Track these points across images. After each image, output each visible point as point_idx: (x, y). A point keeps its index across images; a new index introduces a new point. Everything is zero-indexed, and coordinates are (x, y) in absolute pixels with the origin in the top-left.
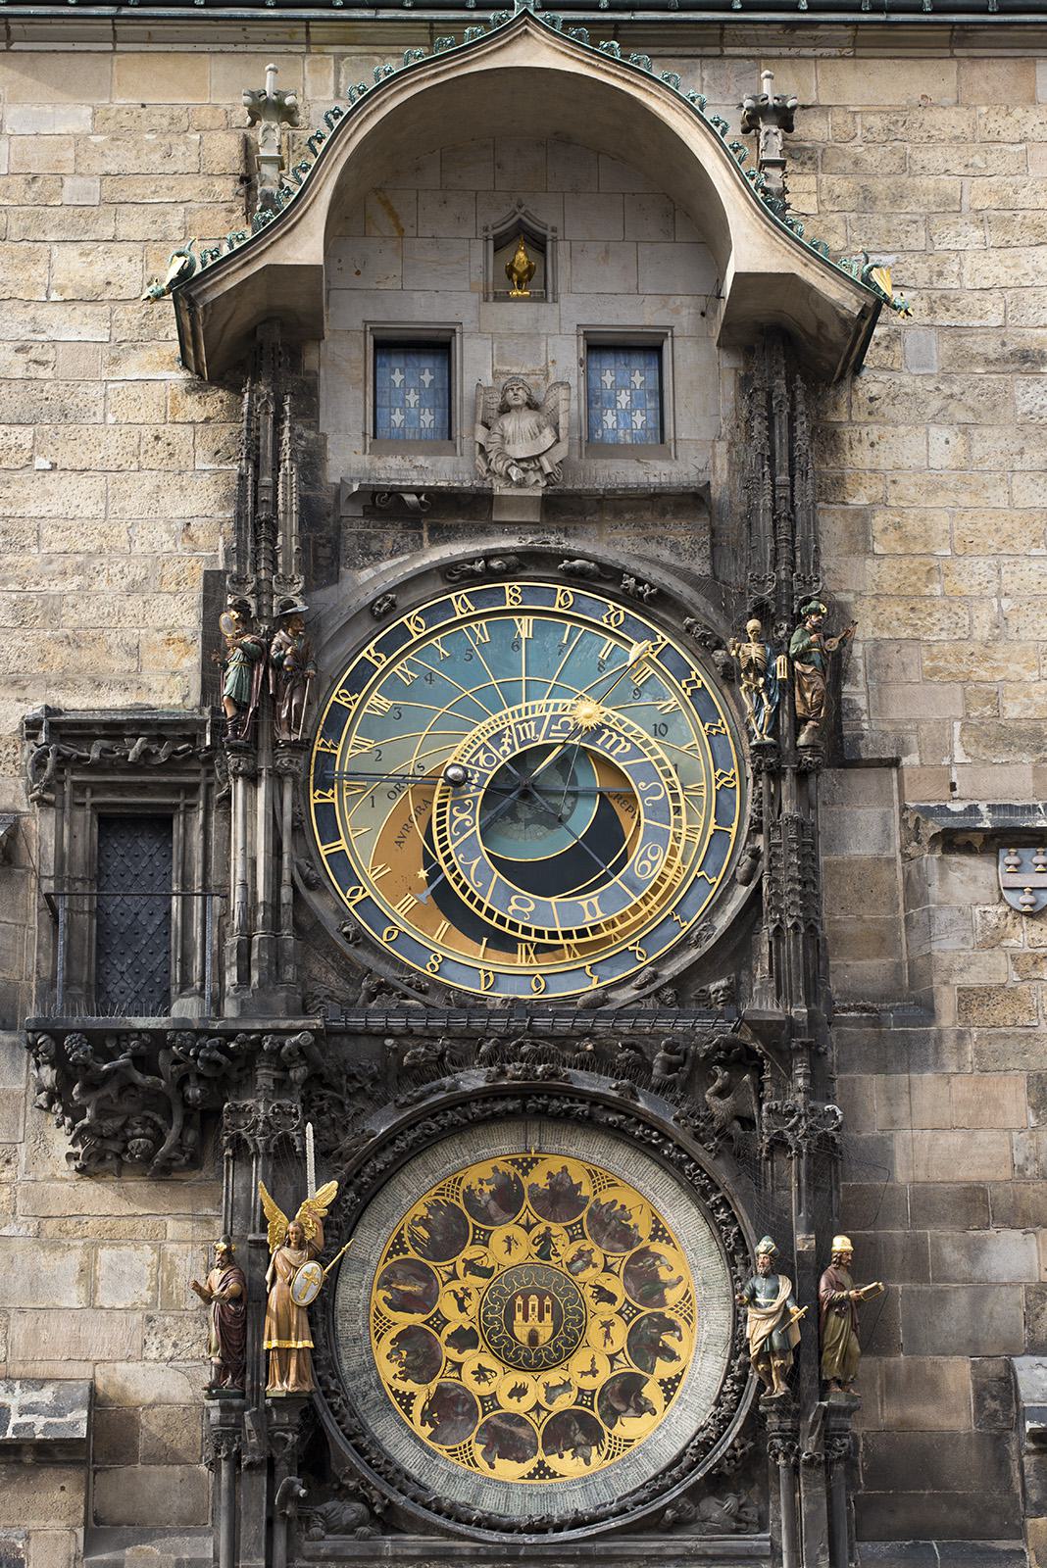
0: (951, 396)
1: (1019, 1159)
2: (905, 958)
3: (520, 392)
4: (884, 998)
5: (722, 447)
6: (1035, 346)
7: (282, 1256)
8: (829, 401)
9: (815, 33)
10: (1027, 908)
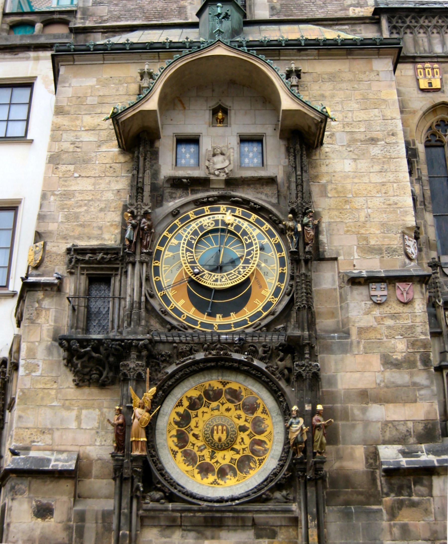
0: (351, 151)
1: (378, 381)
6: (375, 136)
7: (138, 411)
8: (313, 153)
10: (379, 302)
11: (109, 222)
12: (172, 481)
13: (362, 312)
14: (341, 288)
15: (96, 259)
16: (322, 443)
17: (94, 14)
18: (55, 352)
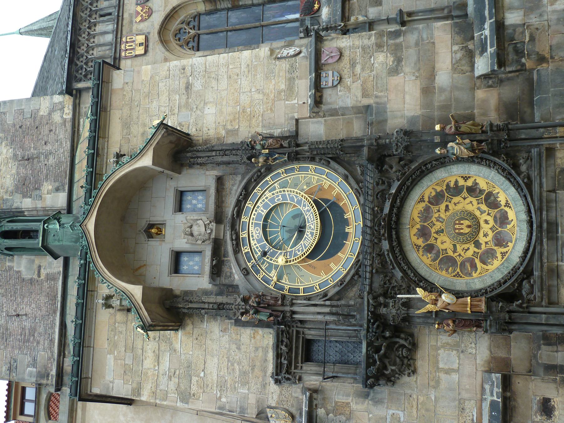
0: (197, 108)
5: (208, 173)
6: (184, 85)
11: (251, 341)
13: (348, 95)
14: (324, 116)
16: (473, 125)
17: (45, 366)
18: (379, 396)
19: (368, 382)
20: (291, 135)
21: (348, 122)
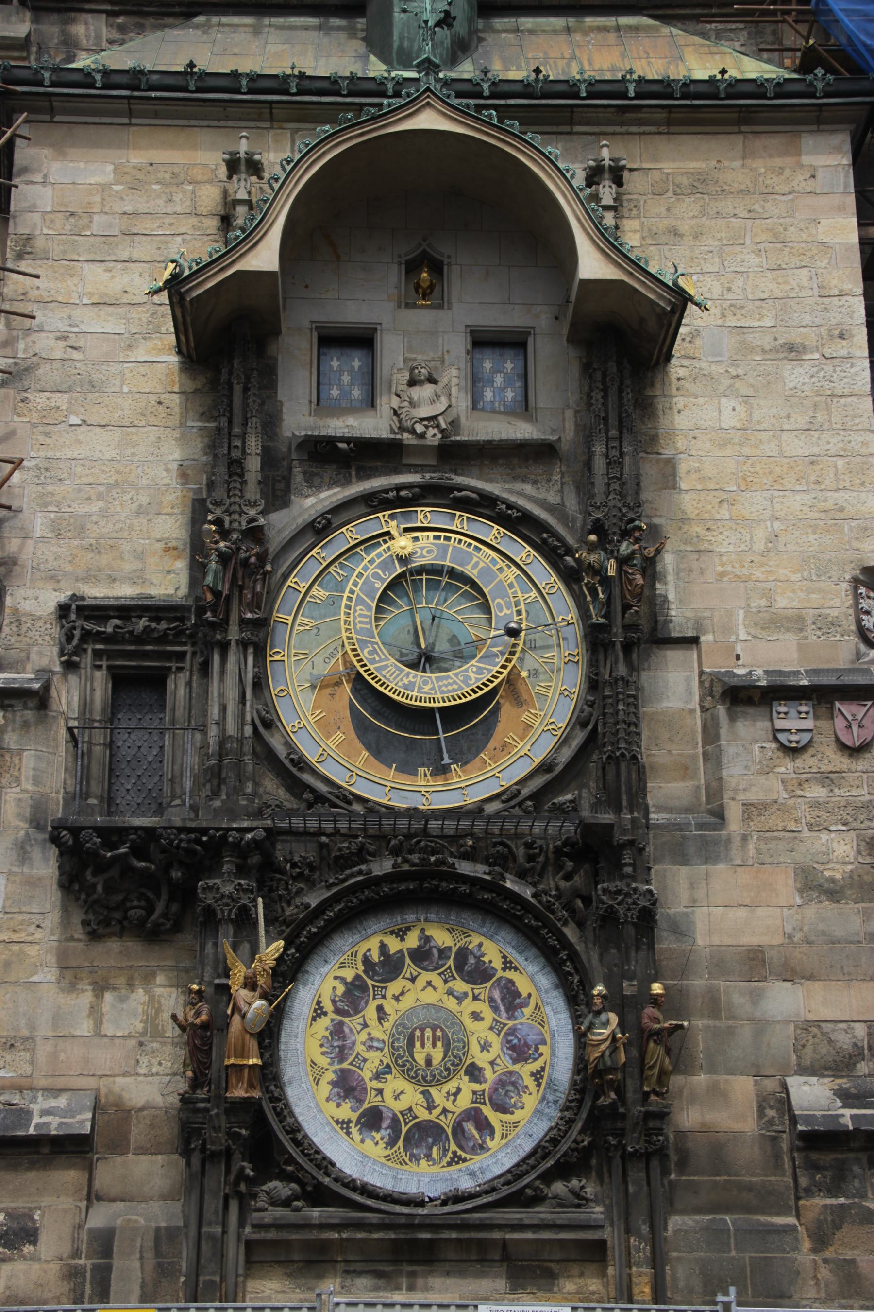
0: (737, 376)
1: (788, 929)
2: (703, 781)
3: (423, 371)
4: (688, 810)
5: (569, 414)
6: (798, 340)
9: (640, 115)
10: (794, 745)
11: (159, 541)
12: (319, 1157)
14: (704, 709)
15: (131, 632)
18: (36, 854)
19: (64, 833)
20: (659, 627)
21: (687, 768)
